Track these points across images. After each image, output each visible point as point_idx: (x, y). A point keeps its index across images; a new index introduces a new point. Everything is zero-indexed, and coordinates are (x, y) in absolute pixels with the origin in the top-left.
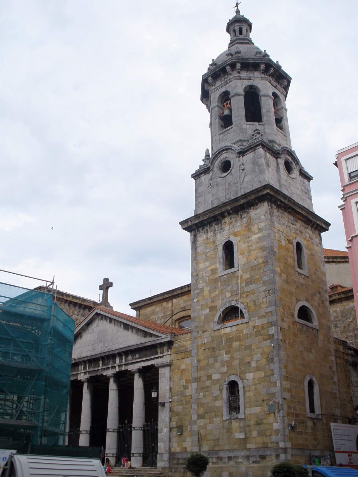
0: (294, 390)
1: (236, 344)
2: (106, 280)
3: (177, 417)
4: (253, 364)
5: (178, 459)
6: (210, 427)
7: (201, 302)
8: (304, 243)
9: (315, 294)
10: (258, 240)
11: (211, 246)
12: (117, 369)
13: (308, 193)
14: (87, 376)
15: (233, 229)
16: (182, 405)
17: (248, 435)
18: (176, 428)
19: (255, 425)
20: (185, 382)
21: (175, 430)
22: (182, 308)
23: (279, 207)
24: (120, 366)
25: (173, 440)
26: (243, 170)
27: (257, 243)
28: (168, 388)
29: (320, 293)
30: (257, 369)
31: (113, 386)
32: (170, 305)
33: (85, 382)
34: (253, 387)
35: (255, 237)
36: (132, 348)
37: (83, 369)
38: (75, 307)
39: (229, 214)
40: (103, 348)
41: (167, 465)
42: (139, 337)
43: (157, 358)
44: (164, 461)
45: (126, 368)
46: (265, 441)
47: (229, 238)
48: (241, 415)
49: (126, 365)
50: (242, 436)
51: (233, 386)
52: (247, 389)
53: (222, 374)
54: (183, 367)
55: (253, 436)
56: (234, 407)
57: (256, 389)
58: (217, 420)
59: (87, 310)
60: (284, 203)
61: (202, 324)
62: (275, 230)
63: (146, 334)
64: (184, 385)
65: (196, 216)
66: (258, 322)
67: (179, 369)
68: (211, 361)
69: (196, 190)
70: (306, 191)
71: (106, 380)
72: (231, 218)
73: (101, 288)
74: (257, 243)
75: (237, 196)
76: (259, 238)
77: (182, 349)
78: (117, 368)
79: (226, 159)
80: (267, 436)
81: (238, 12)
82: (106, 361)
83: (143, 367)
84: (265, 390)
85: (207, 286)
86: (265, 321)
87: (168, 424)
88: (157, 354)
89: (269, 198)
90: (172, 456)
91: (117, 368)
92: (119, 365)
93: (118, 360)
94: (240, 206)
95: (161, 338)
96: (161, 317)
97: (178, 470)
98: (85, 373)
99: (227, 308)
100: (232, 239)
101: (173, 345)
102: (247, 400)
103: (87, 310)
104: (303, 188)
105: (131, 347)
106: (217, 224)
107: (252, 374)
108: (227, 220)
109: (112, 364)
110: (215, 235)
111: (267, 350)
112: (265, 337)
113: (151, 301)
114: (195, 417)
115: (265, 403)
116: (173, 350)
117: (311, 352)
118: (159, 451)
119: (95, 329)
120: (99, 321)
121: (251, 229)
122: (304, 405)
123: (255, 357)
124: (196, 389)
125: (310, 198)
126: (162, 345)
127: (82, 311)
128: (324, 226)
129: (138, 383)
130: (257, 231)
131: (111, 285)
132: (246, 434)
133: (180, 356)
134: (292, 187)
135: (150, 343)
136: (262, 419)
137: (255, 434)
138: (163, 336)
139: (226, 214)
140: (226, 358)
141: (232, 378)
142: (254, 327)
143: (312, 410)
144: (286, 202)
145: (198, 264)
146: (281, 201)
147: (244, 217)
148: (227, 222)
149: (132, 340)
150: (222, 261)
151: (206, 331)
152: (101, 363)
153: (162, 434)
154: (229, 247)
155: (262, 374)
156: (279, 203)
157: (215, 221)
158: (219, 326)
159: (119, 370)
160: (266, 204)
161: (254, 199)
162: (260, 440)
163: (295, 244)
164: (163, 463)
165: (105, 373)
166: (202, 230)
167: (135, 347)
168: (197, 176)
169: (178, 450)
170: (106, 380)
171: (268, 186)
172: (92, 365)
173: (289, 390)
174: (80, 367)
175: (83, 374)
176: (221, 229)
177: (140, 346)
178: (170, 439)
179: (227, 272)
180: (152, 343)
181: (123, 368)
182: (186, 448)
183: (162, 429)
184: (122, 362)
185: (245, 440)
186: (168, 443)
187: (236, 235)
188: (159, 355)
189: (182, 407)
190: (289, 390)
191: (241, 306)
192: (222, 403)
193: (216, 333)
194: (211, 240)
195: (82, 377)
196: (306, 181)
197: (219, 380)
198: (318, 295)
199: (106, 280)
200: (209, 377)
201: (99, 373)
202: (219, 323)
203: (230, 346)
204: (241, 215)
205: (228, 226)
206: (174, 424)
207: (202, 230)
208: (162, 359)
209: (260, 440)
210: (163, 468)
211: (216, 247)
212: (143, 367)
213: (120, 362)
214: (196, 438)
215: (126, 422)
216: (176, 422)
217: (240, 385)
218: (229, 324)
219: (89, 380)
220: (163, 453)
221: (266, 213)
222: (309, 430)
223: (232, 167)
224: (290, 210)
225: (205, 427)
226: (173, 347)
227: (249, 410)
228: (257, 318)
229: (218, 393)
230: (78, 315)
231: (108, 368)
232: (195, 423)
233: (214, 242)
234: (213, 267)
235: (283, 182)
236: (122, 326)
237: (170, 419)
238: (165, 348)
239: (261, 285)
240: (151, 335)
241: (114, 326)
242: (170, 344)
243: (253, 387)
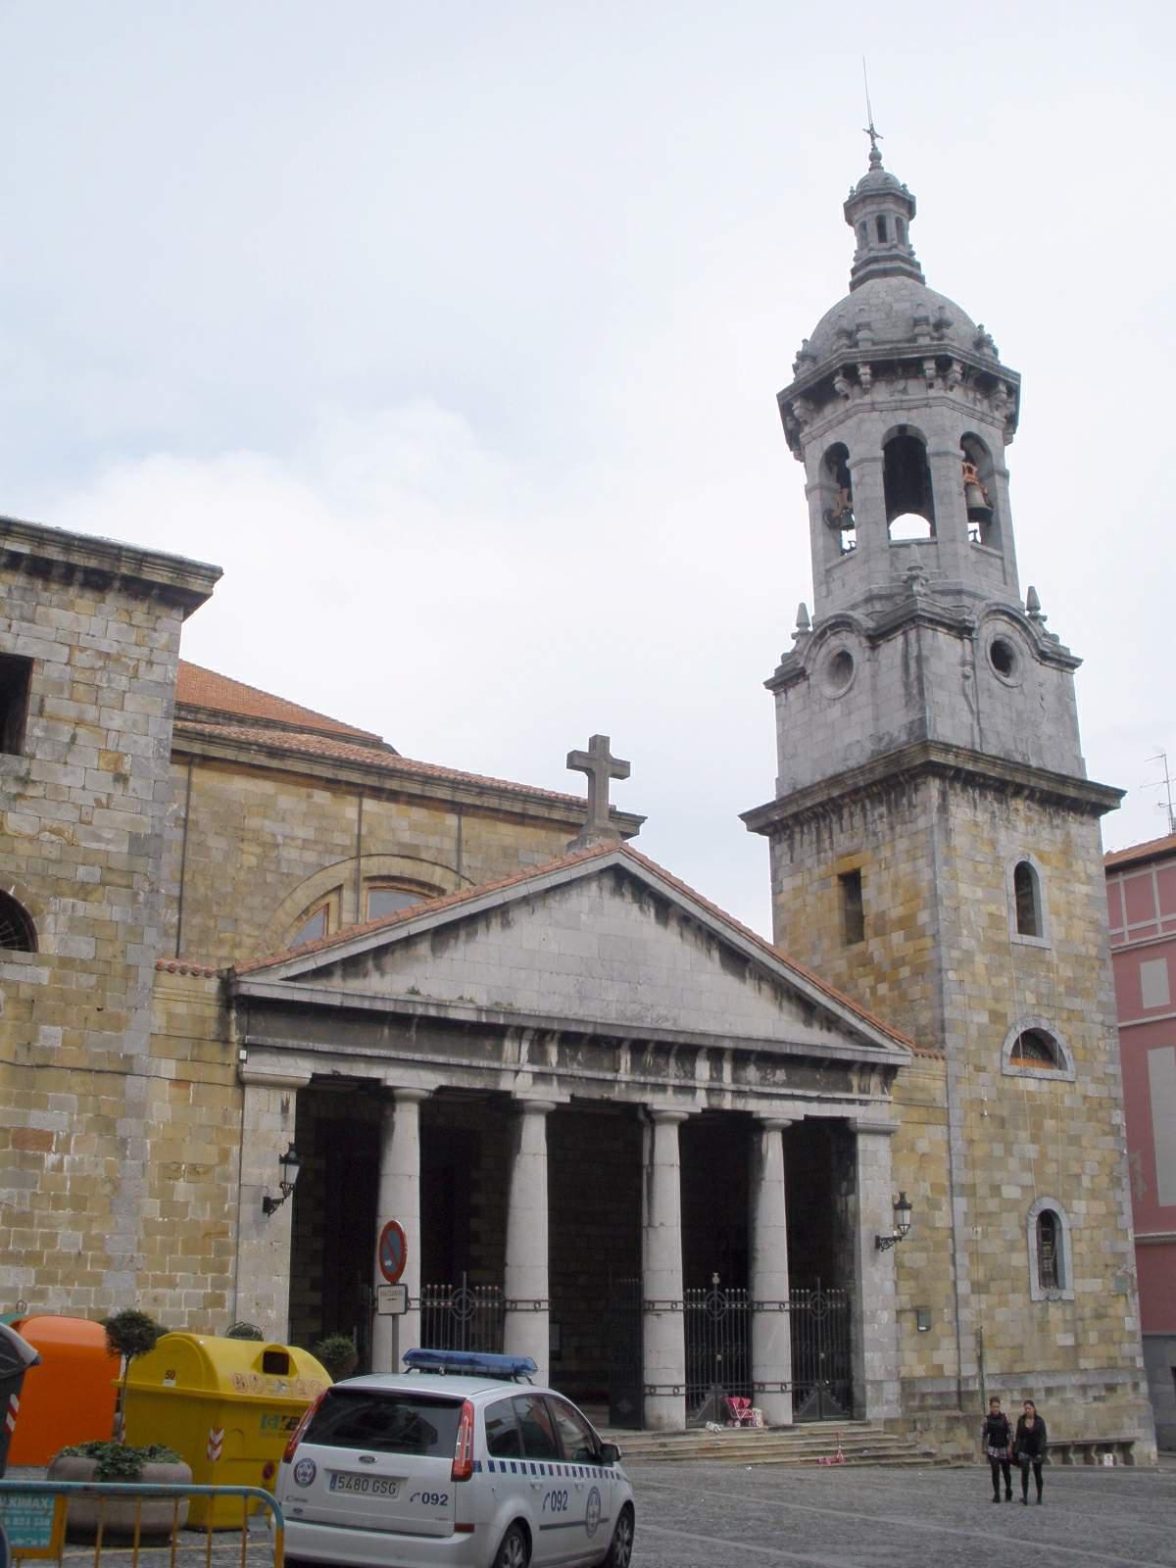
1: (1050, 1124)
3: (912, 1283)
4: (1086, 1181)
5: (923, 1396)
12: (700, 1102)
14: (556, 1095)
16: (925, 1249)
18: (910, 1311)
20: (932, 1190)
21: (911, 1316)
22: (400, 844)
30: (1094, 1194)
33: (538, 1111)
34: (1087, 1233)
37: (524, 1056)
39: (1031, 797)
40: (633, 1006)
41: (896, 1412)
42: (785, 1017)
44: (888, 1402)
45: (741, 1105)
48: (1067, 1295)
49: (738, 1094)
50: (1069, 1341)
53: (1024, 1187)
54: (923, 1146)
56: (1051, 1275)
57: (1092, 1239)
58: (1018, 1299)
64: (928, 1199)
66: (1092, 1090)
67: (912, 1149)
68: (998, 1150)
77: (919, 1096)
78: (701, 1095)
79: (1007, 641)
80: (1115, 1343)
81: (875, 157)
83: (806, 1117)
88: (849, 1089)
90: (907, 1385)
91: (701, 1095)
95: (882, 1050)
96: (304, 840)
97: (933, 1425)
98: (539, 1077)
100: (1034, 862)
101: (894, 1078)
105: (783, 1045)
107: (1083, 1203)
109: (677, 1077)
112: (1107, 1128)
113: (275, 764)
114: (964, 1287)
115: (1110, 1271)
116: (894, 1089)
118: (869, 1376)
119: (583, 917)
120: (606, 895)
124: (965, 1214)
126: (868, 1068)
132: (1076, 1336)
133: (915, 1114)
135: (850, 1053)
136: (1104, 1307)
140: (1031, 1151)
141: (1048, 1204)
149: (759, 1018)
152: (625, 1059)
153: (876, 1326)
155: (1100, 1208)
159: (709, 1103)
164: (885, 1408)
169: (920, 1371)
172: (580, 1057)
174: (509, 1046)
176: (1008, 820)
178: (898, 1341)
181: (728, 1103)
182: (940, 1367)
183: (874, 1314)
184: (720, 1079)
189: (924, 1255)
192: (1026, 1259)
193: (1007, 1084)
195: (520, 1085)
200: (995, 1190)
201: (617, 1094)
203: (1038, 1126)
208: (864, 1108)
210: (890, 1423)
213: (712, 1078)
214: (968, 1342)
215: (716, 1280)
216: (912, 1296)
220: (881, 1381)
226: (894, 1082)
228: (1088, 1079)
229: (1016, 1233)
231: (662, 1088)
238: (875, 1081)
240: (831, 1022)
241: (679, 939)
242: (889, 1072)
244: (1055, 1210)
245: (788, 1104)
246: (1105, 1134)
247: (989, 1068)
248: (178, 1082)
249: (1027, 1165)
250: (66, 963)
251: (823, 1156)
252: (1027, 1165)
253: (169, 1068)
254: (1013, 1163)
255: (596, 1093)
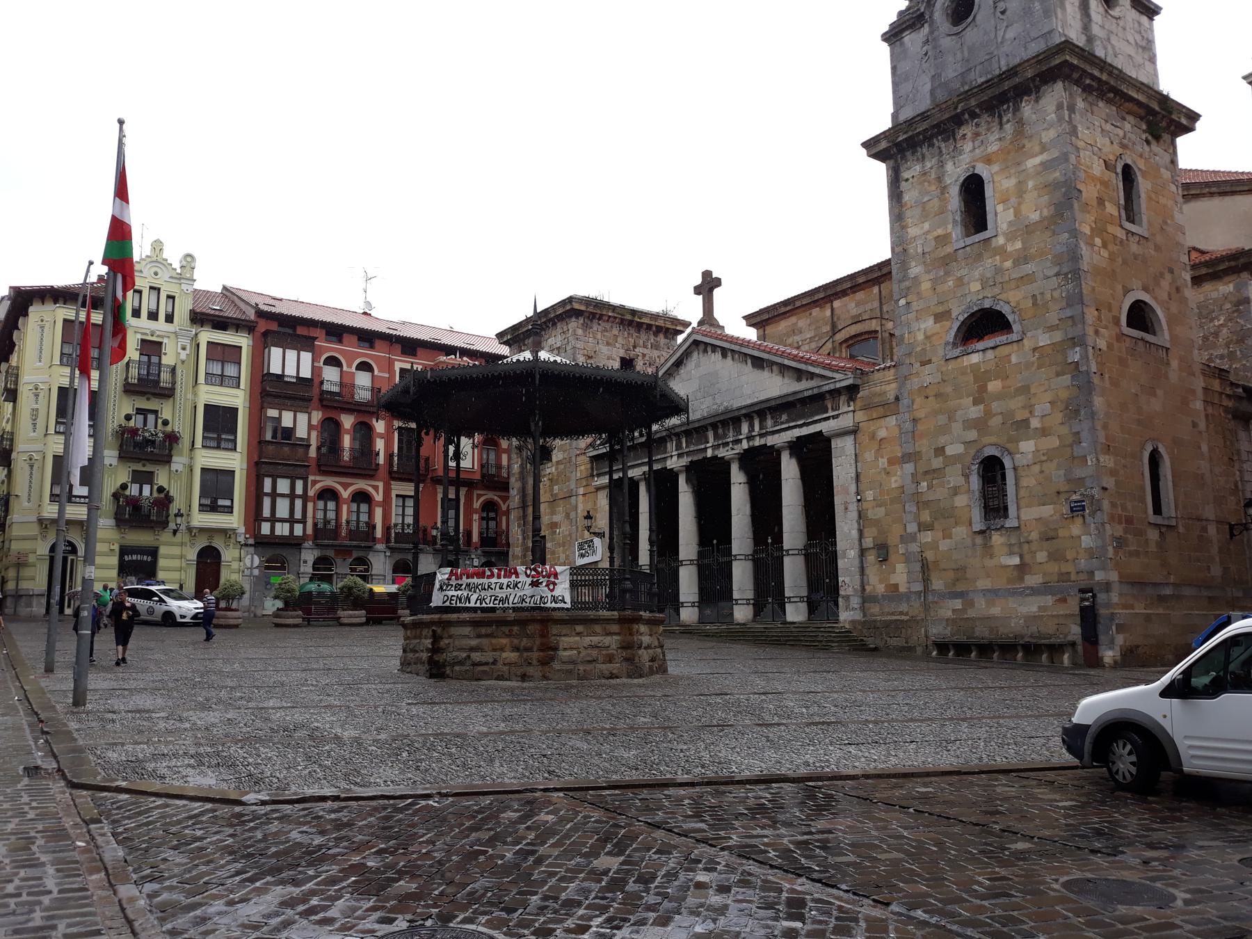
0: (1122, 472)
1: (994, 386)
2: (707, 275)
4: (1035, 423)
6: (944, 545)
7: (915, 306)
8: (1139, 165)
9: (1162, 275)
10: (1040, 169)
11: (934, 188)
12: (745, 445)
13: (1147, 47)
14: (685, 461)
15: (982, 148)
17: (1027, 558)
19: (1041, 539)
21: (873, 552)
22: (853, 317)
23: (1087, 89)
24: (749, 438)
25: (868, 571)
26: (1003, 13)
27: (1038, 174)
28: (853, 475)
29: (1171, 271)
30: (1044, 432)
31: (738, 478)
32: (828, 313)
34: (1036, 468)
35: (1032, 163)
36: (773, 403)
38: (639, 332)
39: (973, 115)
42: (787, 380)
43: (828, 418)
44: (853, 609)
45: (763, 442)
46: (1064, 570)
47: (974, 167)
48: (1010, 523)
49: (761, 435)
50: (1016, 560)
51: (992, 470)
52: (1021, 472)
54: (882, 433)
55: (1039, 560)
57: (1042, 472)
58: (960, 532)
59: (661, 336)
60: (1099, 80)
61: (918, 349)
62: (1081, 144)
63: (799, 374)
65: (897, 127)
66: (1044, 340)
67: (873, 436)
69: (894, 69)
70: (1144, 43)
71: (724, 465)
72: (977, 125)
73: (698, 290)
74: (1038, 174)
75: (989, 76)
76: (1042, 164)
78: (745, 442)
82: (720, 431)
84: (1062, 472)
85: (928, 272)
86: (1058, 336)
87: (857, 542)
89: (1066, 70)
91: (745, 442)
92: (747, 437)
93: (745, 428)
94: (1002, 95)
98: (679, 456)
99: (973, 314)
100: (982, 170)
102: (1022, 493)
103: (661, 336)
104: (1138, 38)
106: (945, 140)
107: (1032, 442)
108: (967, 130)
110: (941, 165)
111: (1064, 395)
114: (912, 528)
117: (1155, 395)
121: (1024, 146)
122: (1143, 501)
123: (1038, 411)
125: (1152, 60)
126: (836, 393)
127: (652, 337)
128: (1184, 121)
129: (790, 469)
130: (1037, 149)
131: (718, 282)
132: (1021, 557)
134: (1114, 40)
136: (1056, 530)
137: (1041, 556)
138: (838, 376)
139: (966, 116)
140: (975, 412)
142: (1035, 350)
143: (1157, 510)
144: (1104, 77)
145: (904, 227)
146: (1093, 77)
147: (1008, 121)
148: (969, 135)
149: (773, 386)
150: (958, 218)
151: (929, 362)
154: (973, 189)
156: (1088, 81)
157: (940, 133)
158: (957, 352)
160: (1059, 86)
161: (1033, 79)
162: (1053, 568)
163: (1119, 170)
165: (722, 453)
166: (913, 153)
167: (779, 402)
168: (895, 35)
169: (881, 589)
170: (724, 465)
171: (1067, 45)
173: (1113, 473)
174: (669, 445)
175: (675, 458)
177: (791, 399)
179: (969, 240)
180: (816, 391)
182: (896, 586)
183: (844, 552)
185: (1022, 568)
186: (858, 577)
187: (988, 160)
188: (831, 413)
190: (1113, 473)
191: (1006, 310)
194: (933, 176)
195: (673, 463)
196: (1144, 19)
197: (960, 455)
198: (1168, 276)
199: (707, 275)
200: (940, 451)
202: (955, 345)
203: (983, 389)
204: (1000, 117)
205: (970, 144)
206: (868, 542)
207: (913, 153)
209: (1053, 568)
211: (944, 190)
212: (798, 438)
217: (1007, 463)
218: (981, 345)
219: (689, 469)
221: (1060, 107)
222: (1153, 548)
223: (976, 7)
224: (1112, 95)
225: (934, 546)
227: (1029, 511)
228: (1040, 331)
229: (961, 480)
230: (645, 346)
231: (727, 444)
232: (913, 538)
233: (939, 179)
234: (940, 232)
235: (1096, 30)
236: (749, 361)
237: (861, 532)
238: (843, 398)
239: (1049, 264)
242: (852, 391)
243: (1036, 468)
244: (997, 454)
245: (789, 432)
246: (1058, 375)
247: (934, 359)
248: (584, 495)
249: (969, 424)
250: (558, 462)
251: (816, 457)
252: (969, 424)
253: (581, 491)
254: (957, 427)
255: (700, 457)
